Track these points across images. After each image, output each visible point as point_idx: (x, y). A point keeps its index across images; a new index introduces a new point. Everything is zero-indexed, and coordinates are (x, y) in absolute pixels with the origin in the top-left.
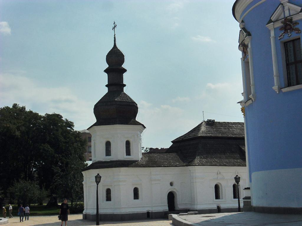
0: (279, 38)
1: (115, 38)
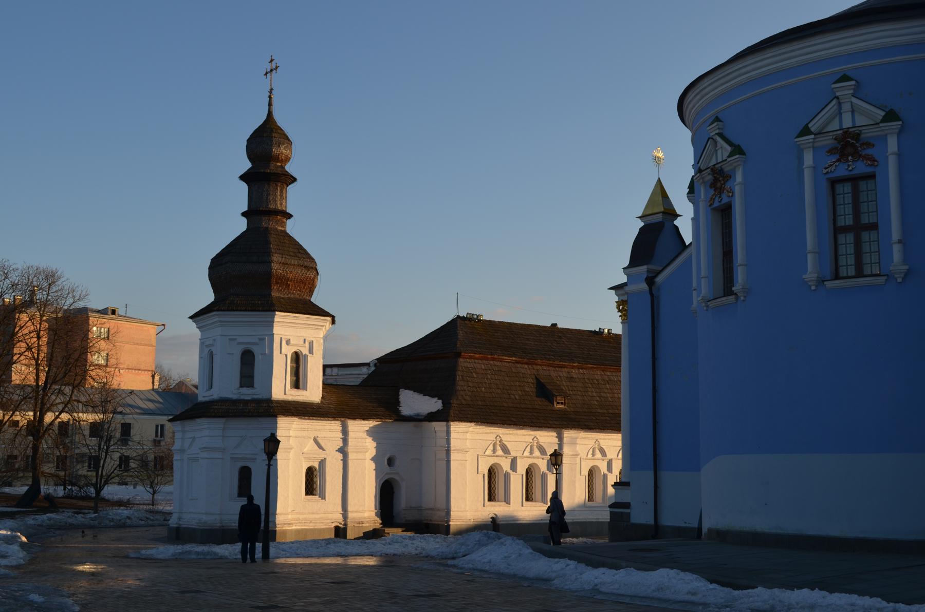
0: (825, 171)
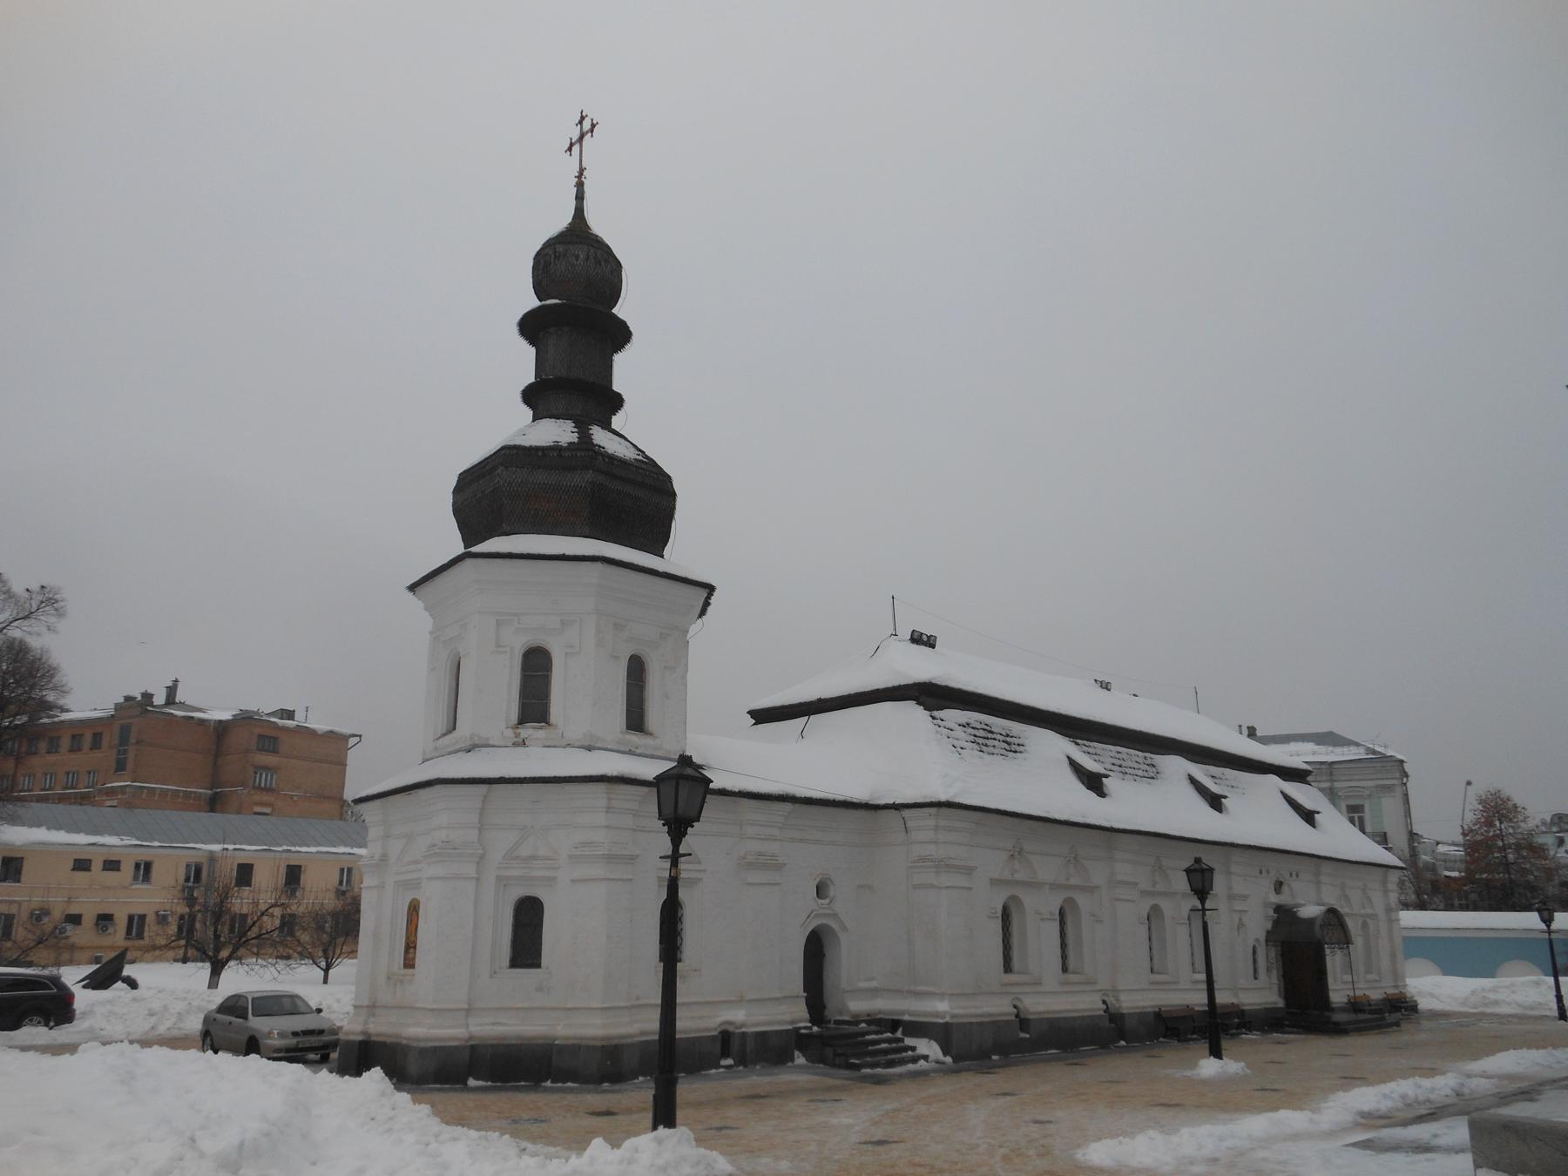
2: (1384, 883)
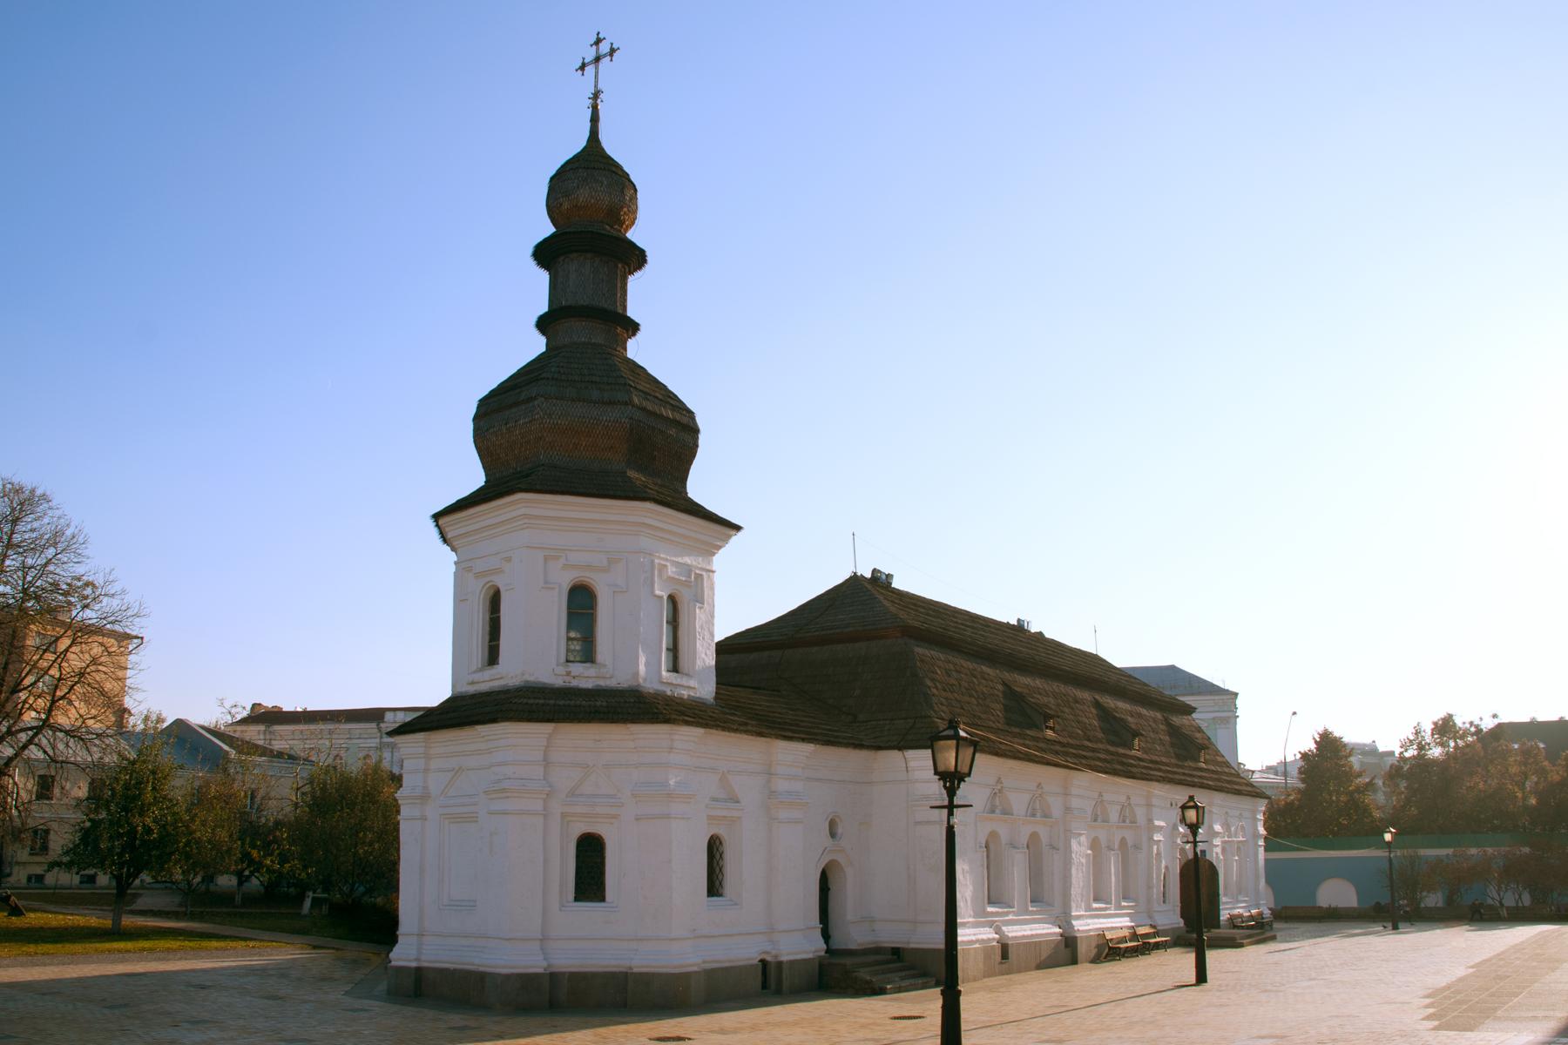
1: (595, 109)
2: (1254, 812)
